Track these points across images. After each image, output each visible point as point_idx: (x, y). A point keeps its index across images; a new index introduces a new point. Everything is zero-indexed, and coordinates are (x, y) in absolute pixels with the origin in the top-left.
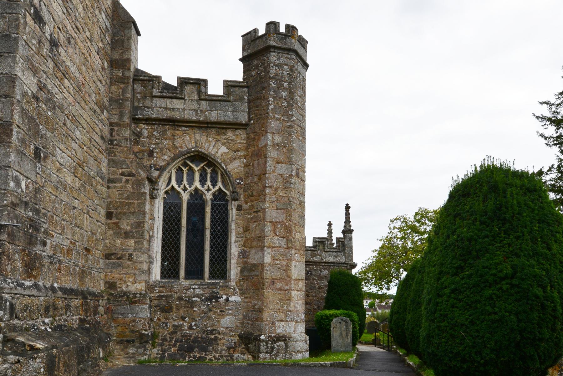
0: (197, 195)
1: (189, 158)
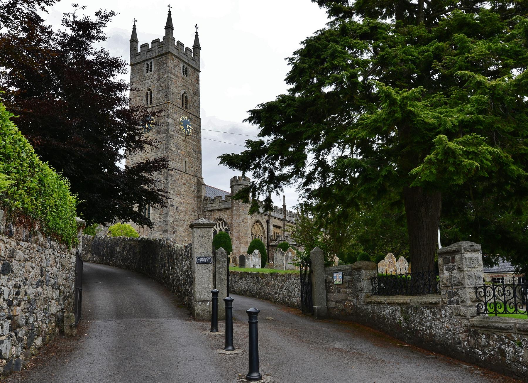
0: (221, 230)
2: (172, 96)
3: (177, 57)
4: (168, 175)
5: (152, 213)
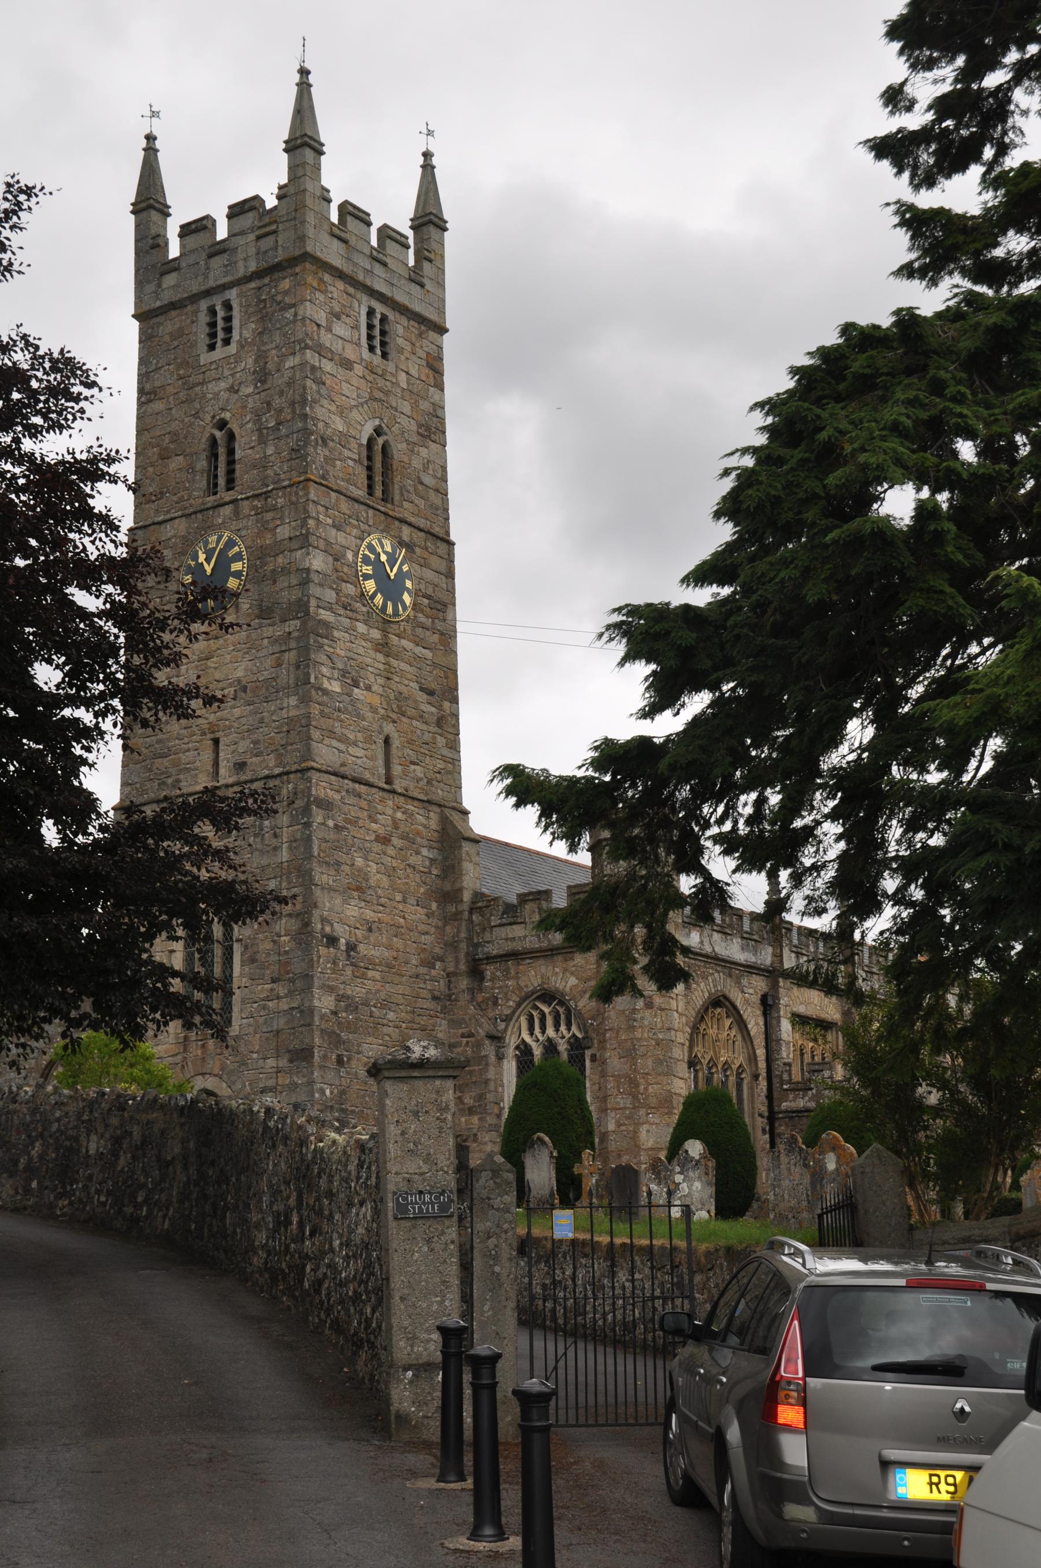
0: (550, 1047)
1: (538, 998)
2: (322, 452)
3: (339, 275)
4: (308, 805)
5: (242, 975)
